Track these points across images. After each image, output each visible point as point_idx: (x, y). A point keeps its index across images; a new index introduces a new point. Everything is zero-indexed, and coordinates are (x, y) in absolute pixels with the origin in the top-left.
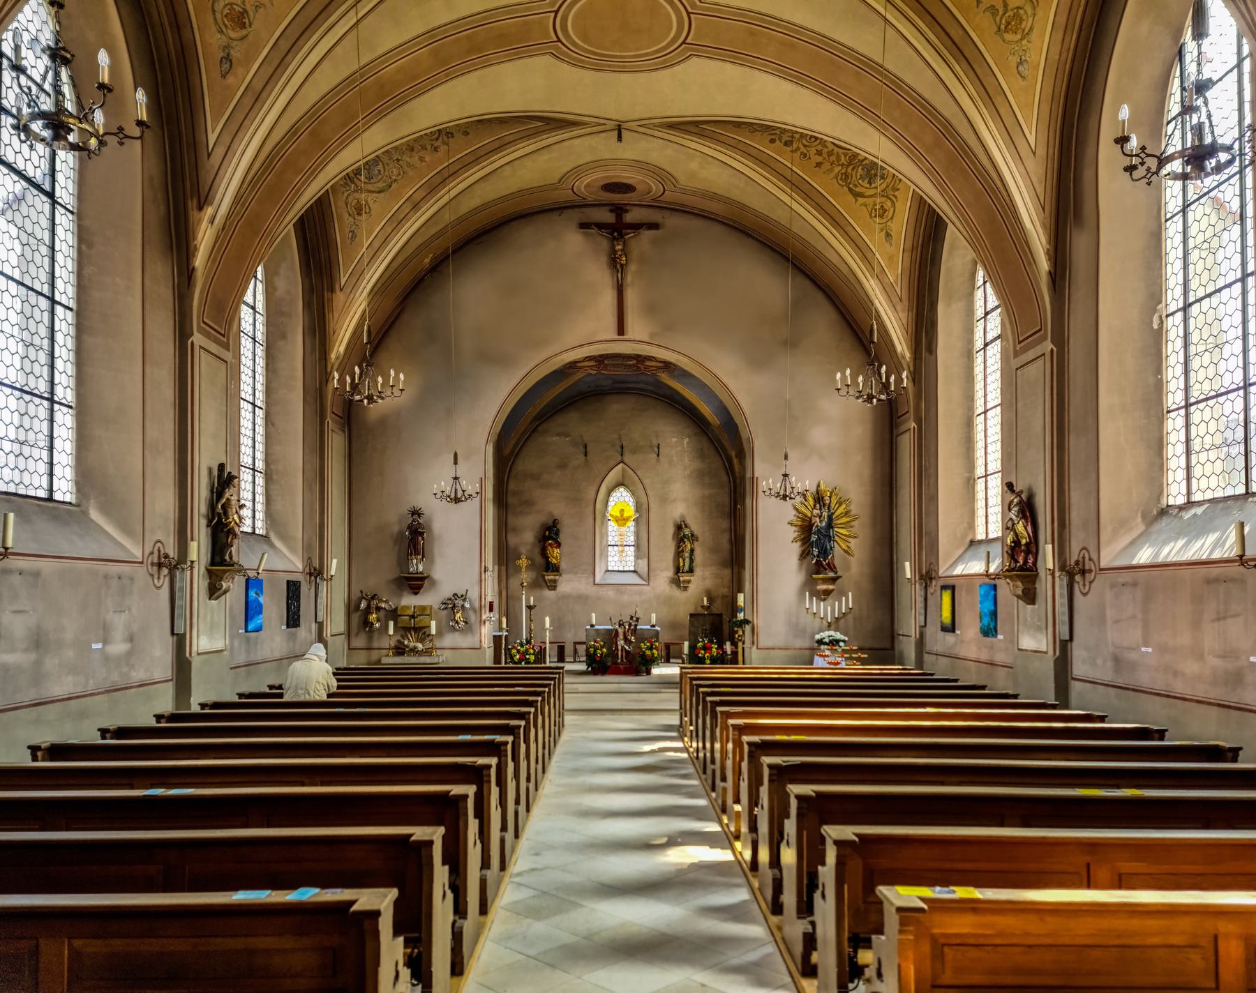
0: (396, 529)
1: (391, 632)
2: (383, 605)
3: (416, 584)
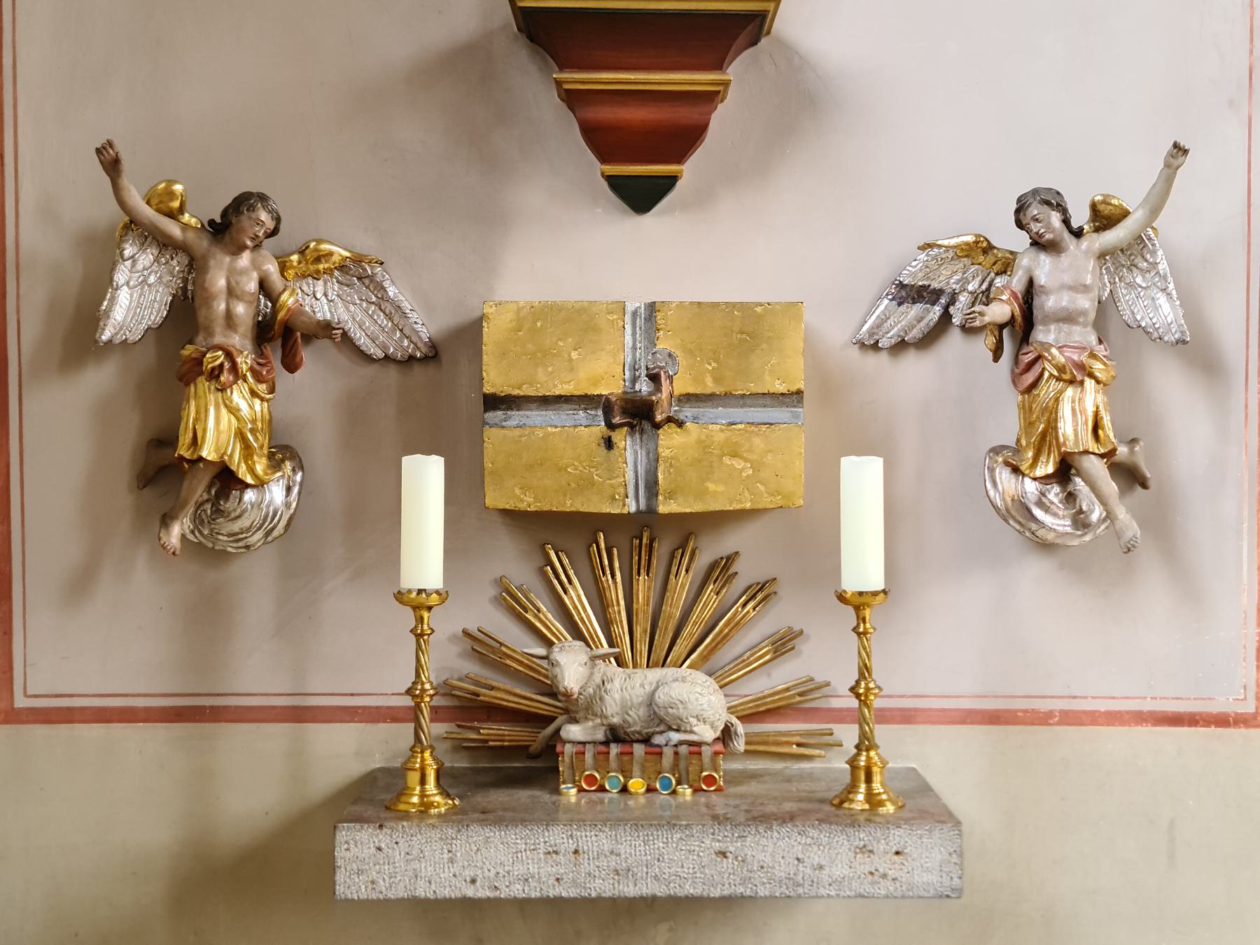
1: (424, 557)
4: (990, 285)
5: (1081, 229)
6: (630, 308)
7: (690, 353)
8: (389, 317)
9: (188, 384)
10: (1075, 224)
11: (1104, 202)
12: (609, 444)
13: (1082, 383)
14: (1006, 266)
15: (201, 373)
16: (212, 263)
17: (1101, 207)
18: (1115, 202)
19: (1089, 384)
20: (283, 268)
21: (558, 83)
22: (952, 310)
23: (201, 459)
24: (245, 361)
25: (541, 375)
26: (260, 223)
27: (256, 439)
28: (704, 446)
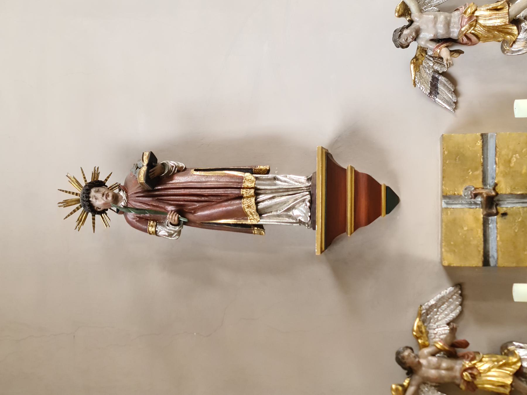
0: (157, 279)
2: (440, 331)
3: (352, 200)
4: (431, 56)
5: (409, 21)
6: (444, 205)
7: (464, 181)
8: (443, 303)
9: (477, 388)
10: (407, 23)
11: (398, 12)
12: (504, 214)
13: (477, 17)
14: (423, 50)
15: (473, 382)
16: (425, 375)
17: (400, 13)
18: (398, 7)
19: (477, 13)
20: (425, 346)
21: (351, 233)
22: (440, 72)
23: (511, 384)
24: (467, 364)
25: (475, 242)
26: (409, 355)
27: (501, 361)
28: (505, 175)
